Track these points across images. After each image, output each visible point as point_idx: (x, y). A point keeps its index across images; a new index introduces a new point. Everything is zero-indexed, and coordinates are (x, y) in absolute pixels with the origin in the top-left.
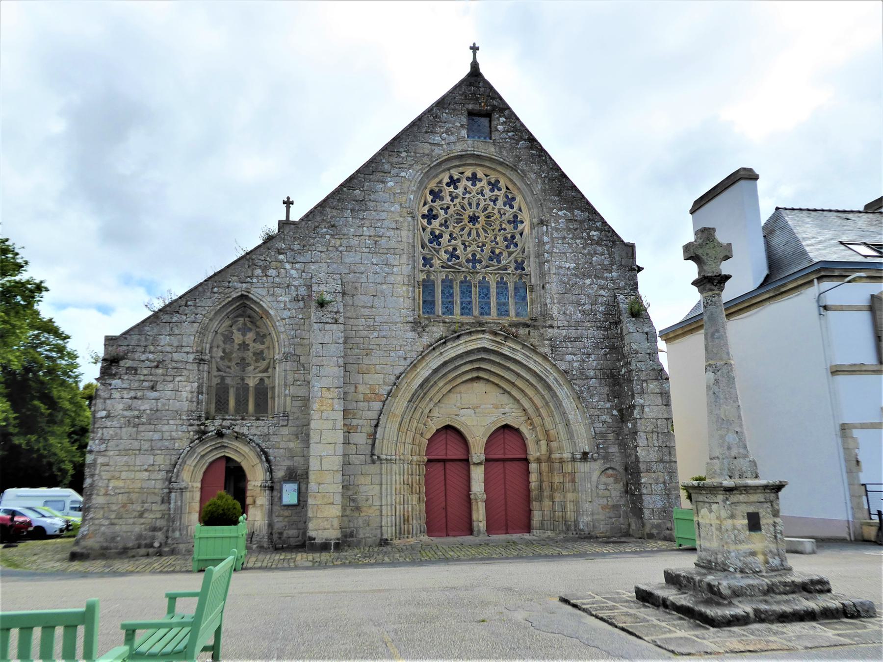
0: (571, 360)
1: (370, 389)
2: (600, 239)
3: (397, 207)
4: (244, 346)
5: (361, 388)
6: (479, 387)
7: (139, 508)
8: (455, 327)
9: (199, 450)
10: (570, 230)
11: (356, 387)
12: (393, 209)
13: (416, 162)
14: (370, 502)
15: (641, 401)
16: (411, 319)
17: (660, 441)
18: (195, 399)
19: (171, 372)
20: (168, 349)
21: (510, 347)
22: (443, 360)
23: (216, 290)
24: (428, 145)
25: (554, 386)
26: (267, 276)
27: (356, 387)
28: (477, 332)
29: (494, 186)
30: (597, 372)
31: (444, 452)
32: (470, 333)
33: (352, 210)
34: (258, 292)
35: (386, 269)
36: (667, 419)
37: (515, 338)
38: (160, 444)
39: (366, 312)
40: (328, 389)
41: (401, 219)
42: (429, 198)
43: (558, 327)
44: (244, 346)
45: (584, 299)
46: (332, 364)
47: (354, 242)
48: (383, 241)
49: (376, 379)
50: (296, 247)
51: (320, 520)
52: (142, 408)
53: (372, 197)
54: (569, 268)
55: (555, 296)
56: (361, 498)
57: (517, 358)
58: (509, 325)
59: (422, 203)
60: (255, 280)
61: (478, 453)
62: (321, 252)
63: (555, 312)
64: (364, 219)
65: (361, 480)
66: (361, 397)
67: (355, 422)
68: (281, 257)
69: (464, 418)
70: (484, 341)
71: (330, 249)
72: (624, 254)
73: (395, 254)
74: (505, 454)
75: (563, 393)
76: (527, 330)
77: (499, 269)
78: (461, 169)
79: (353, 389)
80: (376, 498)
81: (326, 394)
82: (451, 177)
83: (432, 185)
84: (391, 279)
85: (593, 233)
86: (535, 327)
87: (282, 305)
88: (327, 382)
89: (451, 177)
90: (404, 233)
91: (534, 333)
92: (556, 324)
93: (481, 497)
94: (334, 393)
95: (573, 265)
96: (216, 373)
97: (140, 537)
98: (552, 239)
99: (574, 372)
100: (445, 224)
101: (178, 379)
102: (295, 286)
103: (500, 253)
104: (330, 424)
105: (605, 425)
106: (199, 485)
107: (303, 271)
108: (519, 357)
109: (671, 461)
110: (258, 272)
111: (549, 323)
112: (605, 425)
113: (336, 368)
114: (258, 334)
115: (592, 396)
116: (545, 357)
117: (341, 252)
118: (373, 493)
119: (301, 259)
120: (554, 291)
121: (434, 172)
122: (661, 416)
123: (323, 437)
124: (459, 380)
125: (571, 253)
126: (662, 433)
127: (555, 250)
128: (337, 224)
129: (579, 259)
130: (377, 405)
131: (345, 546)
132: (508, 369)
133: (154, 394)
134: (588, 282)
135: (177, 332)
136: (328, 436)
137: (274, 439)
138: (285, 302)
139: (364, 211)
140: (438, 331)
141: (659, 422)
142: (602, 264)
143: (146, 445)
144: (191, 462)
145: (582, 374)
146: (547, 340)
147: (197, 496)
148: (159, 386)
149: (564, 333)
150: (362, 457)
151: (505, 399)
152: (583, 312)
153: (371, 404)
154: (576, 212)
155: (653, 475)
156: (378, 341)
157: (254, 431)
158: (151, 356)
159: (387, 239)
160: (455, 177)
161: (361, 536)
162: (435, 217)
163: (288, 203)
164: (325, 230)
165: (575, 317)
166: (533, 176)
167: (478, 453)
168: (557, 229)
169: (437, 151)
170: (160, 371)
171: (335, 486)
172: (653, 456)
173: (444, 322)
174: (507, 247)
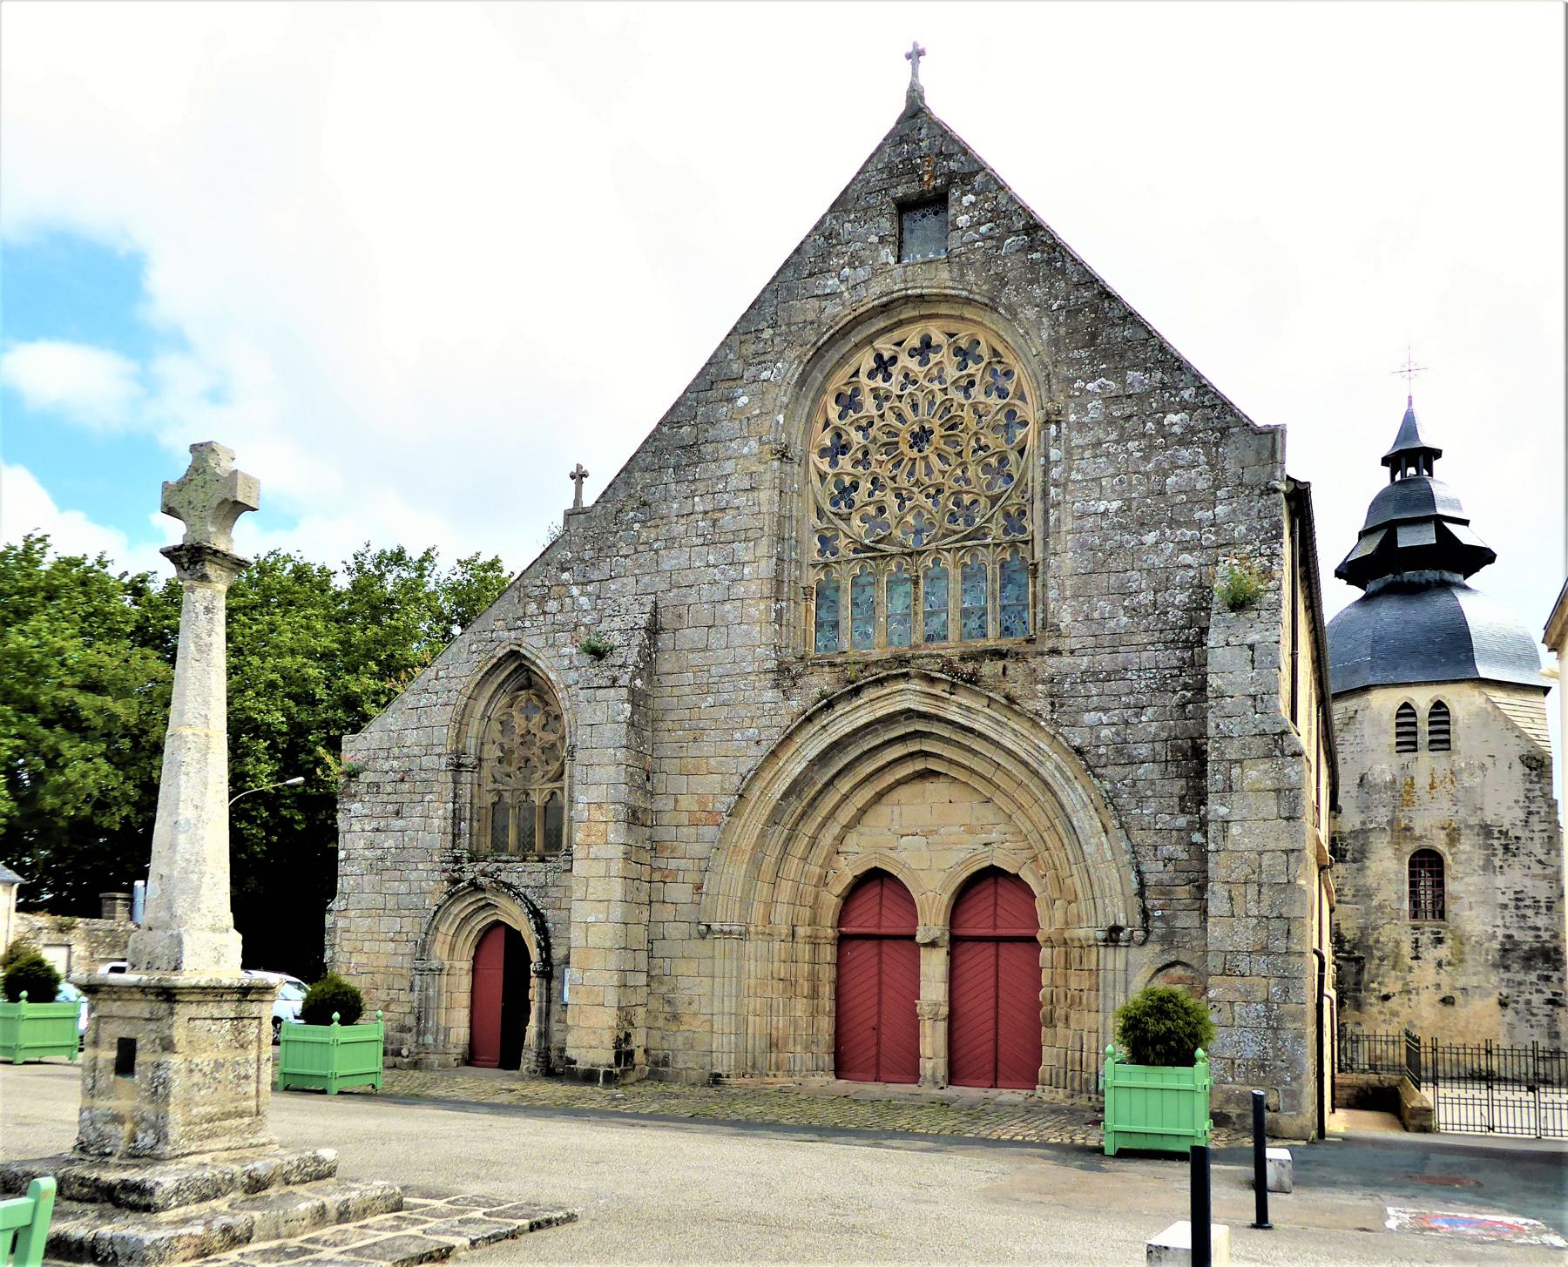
0: (1096, 724)
1: (700, 802)
2: (1191, 430)
3: (753, 443)
4: (527, 738)
5: (686, 802)
7: (384, 997)
8: (851, 673)
9: (455, 909)
10: (1111, 421)
11: (676, 801)
12: (746, 450)
14: (695, 1006)
15: (1223, 811)
18: (449, 829)
19: (420, 788)
20: (416, 751)
21: (960, 705)
22: (829, 741)
23: (474, 647)
25: (1057, 782)
26: (544, 613)
27: (676, 801)
28: (896, 677)
29: (964, 355)
30: (1158, 746)
31: (875, 921)
32: (880, 682)
34: (533, 646)
35: (732, 573)
37: (973, 680)
39: (695, 658)
40: (599, 805)
41: (762, 468)
43: (1072, 652)
45: (1137, 580)
46: (606, 760)
47: (679, 529)
48: (726, 519)
49: (710, 785)
50: (588, 555)
51: (583, 1032)
52: (386, 845)
53: (711, 433)
54: (1105, 513)
55: (1068, 583)
56: (681, 997)
57: (976, 727)
58: (962, 659)
60: (527, 624)
62: (626, 557)
63: (1066, 618)
64: (695, 480)
65: (682, 967)
66: (684, 818)
67: (673, 864)
68: (566, 576)
69: (904, 855)
70: (909, 695)
71: (640, 548)
72: (1250, 456)
73: (747, 540)
74: (995, 927)
76: (1000, 664)
77: (967, 538)
79: (671, 805)
80: (705, 1000)
81: (597, 815)
84: (739, 590)
85: (1171, 418)
86: (1018, 657)
87: (567, 662)
88: (595, 794)
90: (764, 495)
92: (1066, 644)
93: (929, 1015)
94: (608, 813)
96: (491, 786)
99: (1102, 750)
100: (864, 461)
101: (427, 798)
102: (586, 626)
103: (974, 502)
104: (600, 869)
105: (1170, 867)
107: (599, 597)
110: (532, 608)
111: (1049, 644)
112: (1170, 867)
113: (612, 769)
114: (547, 714)
116: (1033, 720)
117: (656, 552)
118: (701, 991)
119: (595, 575)
120: (1067, 570)
123: (590, 890)
124: (889, 779)
125: (1113, 477)
126: (1272, 886)
127: (1075, 476)
128: (650, 499)
131: (633, 1076)
132: (975, 753)
133: (400, 823)
135: (426, 723)
136: (597, 889)
137: (552, 892)
138: (570, 657)
139: (696, 464)
140: (822, 682)
143: (391, 904)
144: (447, 928)
145: (1119, 752)
146: (1043, 682)
150: (684, 926)
152: (1133, 611)
154: (1132, 375)
155: (1238, 981)
156: (715, 713)
157: (526, 880)
158: (395, 763)
159: (735, 512)
161: (680, 1065)
162: (844, 449)
164: (631, 514)
165: (1112, 623)
168: (1081, 427)
170: (406, 787)
171: (608, 974)
172: (1245, 937)
173: (832, 665)
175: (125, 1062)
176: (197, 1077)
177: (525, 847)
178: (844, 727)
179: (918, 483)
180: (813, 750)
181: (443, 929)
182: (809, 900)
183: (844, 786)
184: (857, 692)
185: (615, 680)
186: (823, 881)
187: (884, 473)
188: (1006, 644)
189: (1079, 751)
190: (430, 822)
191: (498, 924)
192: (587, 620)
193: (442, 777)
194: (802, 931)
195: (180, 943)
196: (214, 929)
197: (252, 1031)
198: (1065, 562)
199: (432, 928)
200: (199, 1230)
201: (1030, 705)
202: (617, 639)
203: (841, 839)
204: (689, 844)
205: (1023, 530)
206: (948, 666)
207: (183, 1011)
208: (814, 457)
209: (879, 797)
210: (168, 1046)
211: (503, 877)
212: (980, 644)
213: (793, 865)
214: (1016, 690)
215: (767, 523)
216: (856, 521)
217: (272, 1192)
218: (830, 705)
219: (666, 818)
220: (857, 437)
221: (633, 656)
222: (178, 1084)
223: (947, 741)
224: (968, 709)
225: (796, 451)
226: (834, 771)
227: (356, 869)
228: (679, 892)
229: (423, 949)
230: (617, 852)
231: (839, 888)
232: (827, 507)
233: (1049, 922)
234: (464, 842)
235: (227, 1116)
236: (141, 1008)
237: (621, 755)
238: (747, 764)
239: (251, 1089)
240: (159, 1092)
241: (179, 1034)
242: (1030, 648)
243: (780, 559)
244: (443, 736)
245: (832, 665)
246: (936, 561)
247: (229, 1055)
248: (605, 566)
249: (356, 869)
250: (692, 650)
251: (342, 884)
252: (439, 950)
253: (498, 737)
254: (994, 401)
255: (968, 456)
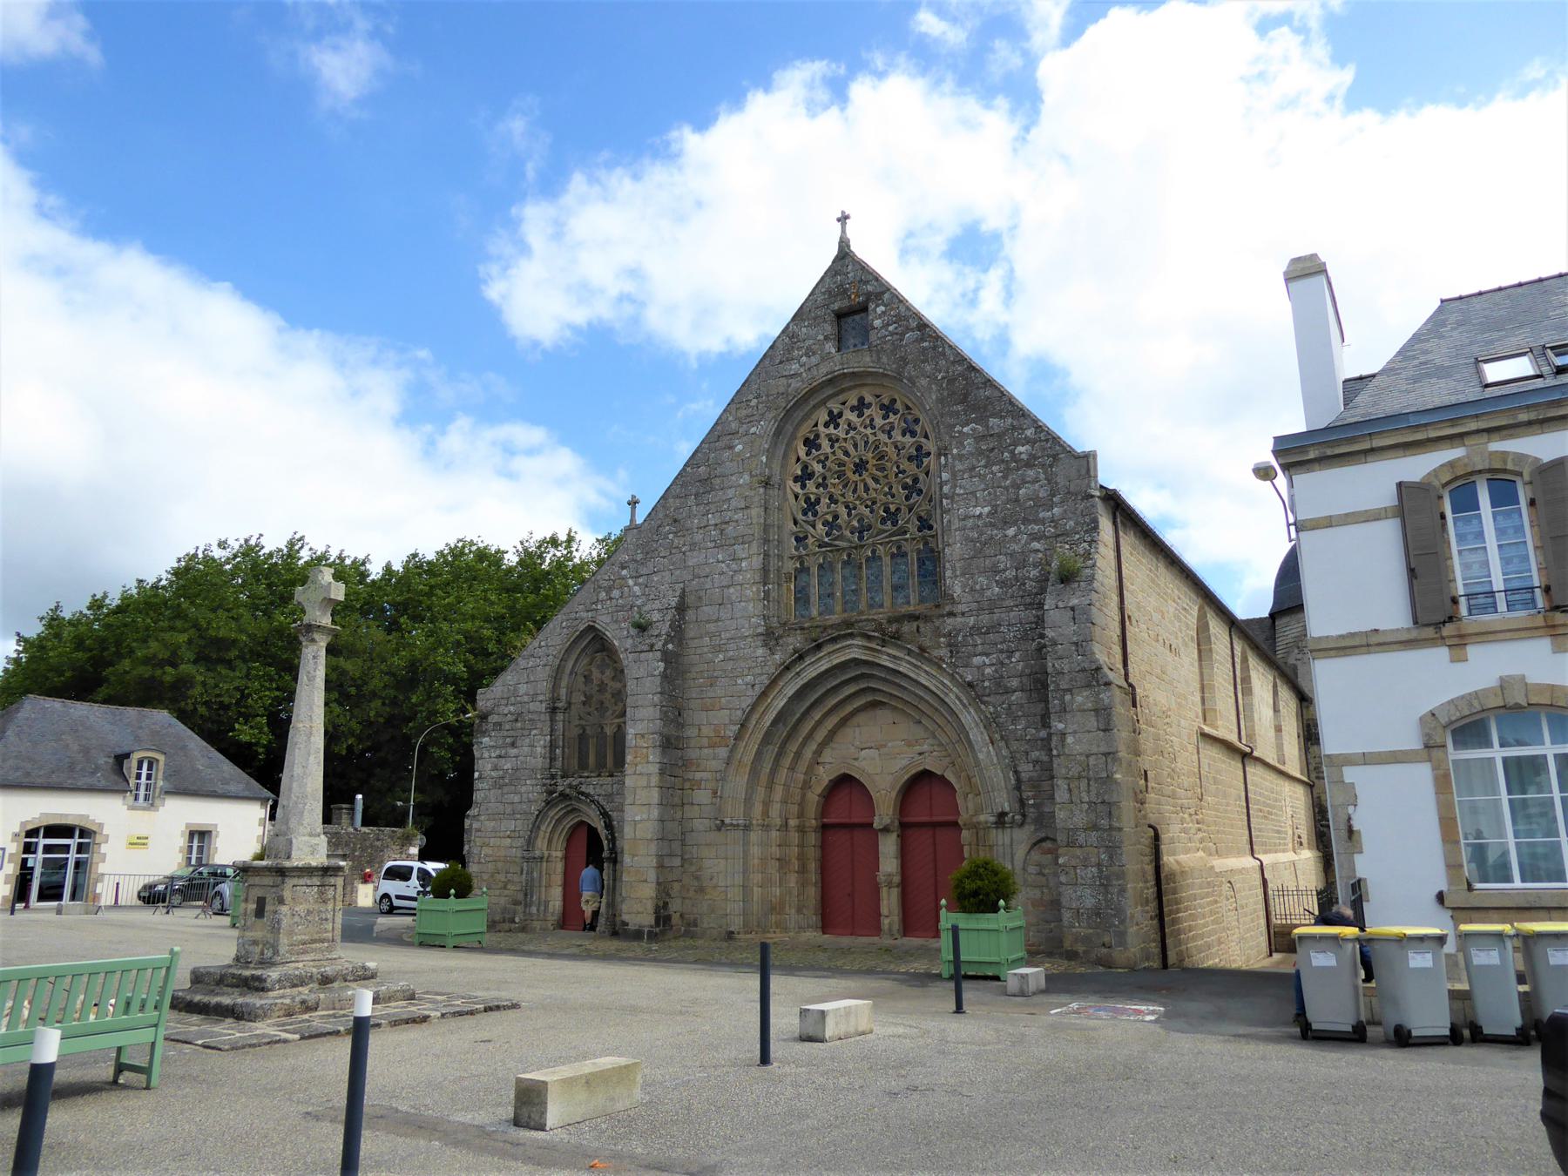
0: (982, 664)
4: (602, 688)
5: (706, 731)
6: (883, 715)
9: (551, 813)
13: (769, 408)
15: (1061, 726)
16: (761, 630)
17: (1093, 792)
20: (526, 699)
24: (784, 381)
25: (957, 706)
30: (1025, 679)
32: (834, 640)
33: (696, 495)
34: (604, 622)
35: (734, 566)
36: (1106, 755)
37: (897, 636)
38: (519, 807)
39: (711, 627)
40: (643, 736)
42: (802, 450)
44: (602, 688)
48: (730, 529)
50: (639, 557)
59: (794, 459)
61: (885, 812)
63: (957, 590)
66: (705, 742)
67: (698, 776)
68: (624, 572)
70: (854, 650)
75: (969, 718)
78: (841, 398)
82: (830, 413)
83: (805, 430)
86: (927, 619)
89: (830, 413)
91: (926, 628)
95: (987, 509)
97: (504, 910)
98: (954, 475)
99: (987, 684)
103: (898, 510)
104: (643, 782)
106: (559, 854)
108: (903, 668)
109: (1111, 828)
111: (947, 609)
114: (615, 669)
115: (1015, 720)
119: (644, 571)
121: (800, 414)
122: (1095, 750)
124: (849, 709)
126: (1096, 780)
129: (996, 497)
130: (723, 752)
133: (513, 752)
134: (1011, 532)
136: (642, 796)
137: (617, 799)
140: (795, 641)
141: (1092, 761)
142: (1036, 499)
145: (998, 685)
147: (560, 867)
148: (519, 743)
149: (972, 621)
151: (919, 732)
153: (718, 750)
155: (1078, 852)
157: (598, 791)
160: (836, 412)
162: (811, 476)
163: (633, 503)
165: (988, 593)
166: (924, 382)
167: (885, 812)
169: (795, 384)
172: (1080, 819)
173: (802, 629)
174: (907, 498)
175: (260, 913)
176: (297, 919)
177: (600, 767)
178: (811, 673)
179: (859, 498)
180: (791, 690)
181: (543, 828)
182: (798, 798)
183: (817, 715)
184: (819, 647)
185: (652, 646)
186: (806, 785)
187: (837, 492)
188: (921, 609)
189: (970, 685)
190: (533, 751)
191: (582, 823)
192: (639, 602)
193: (543, 717)
194: (792, 822)
195: (291, 842)
196: (311, 835)
197: (331, 892)
198: (955, 551)
199: (535, 828)
200: (287, 1001)
201: (936, 653)
202: (656, 616)
203: (818, 752)
204: (709, 760)
205: (930, 528)
206: (879, 627)
207: (290, 882)
208: (790, 483)
209: (844, 722)
210: (281, 901)
211: (583, 788)
212: (905, 609)
213: (783, 774)
214: (927, 643)
215: (757, 531)
216: (820, 526)
217: (336, 985)
218: (801, 658)
219: (693, 743)
220: (818, 468)
221: (665, 628)
222: (285, 922)
223: (885, 680)
224: (895, 657)
225: (776, 479)
226: (808, 704)
227: (485, 786)
228: (702, 796)
229: (530, 843)
230: (654, 769)
231: (819, 790)
232: (800, 517)
233: (967, 808)
234: (559, 764)
235: (314, 941)
236: (268, 881)
237: (657, 698)
238: (747, 702)
239: (330, 927)
240: (275, 928)
241: (287, 894)
242: (938, 612)
243: (766, 555)
244: (544, 686)
245: (802, 629)
246: (874, 552)
247: (316, 907)
248: (650, 565)
249: (485, 786)
250: (708, 622)
251: (478, 796)
252: (541, 844)
253: (582, 687)
254: (908, 439)
255: (892, 479)
